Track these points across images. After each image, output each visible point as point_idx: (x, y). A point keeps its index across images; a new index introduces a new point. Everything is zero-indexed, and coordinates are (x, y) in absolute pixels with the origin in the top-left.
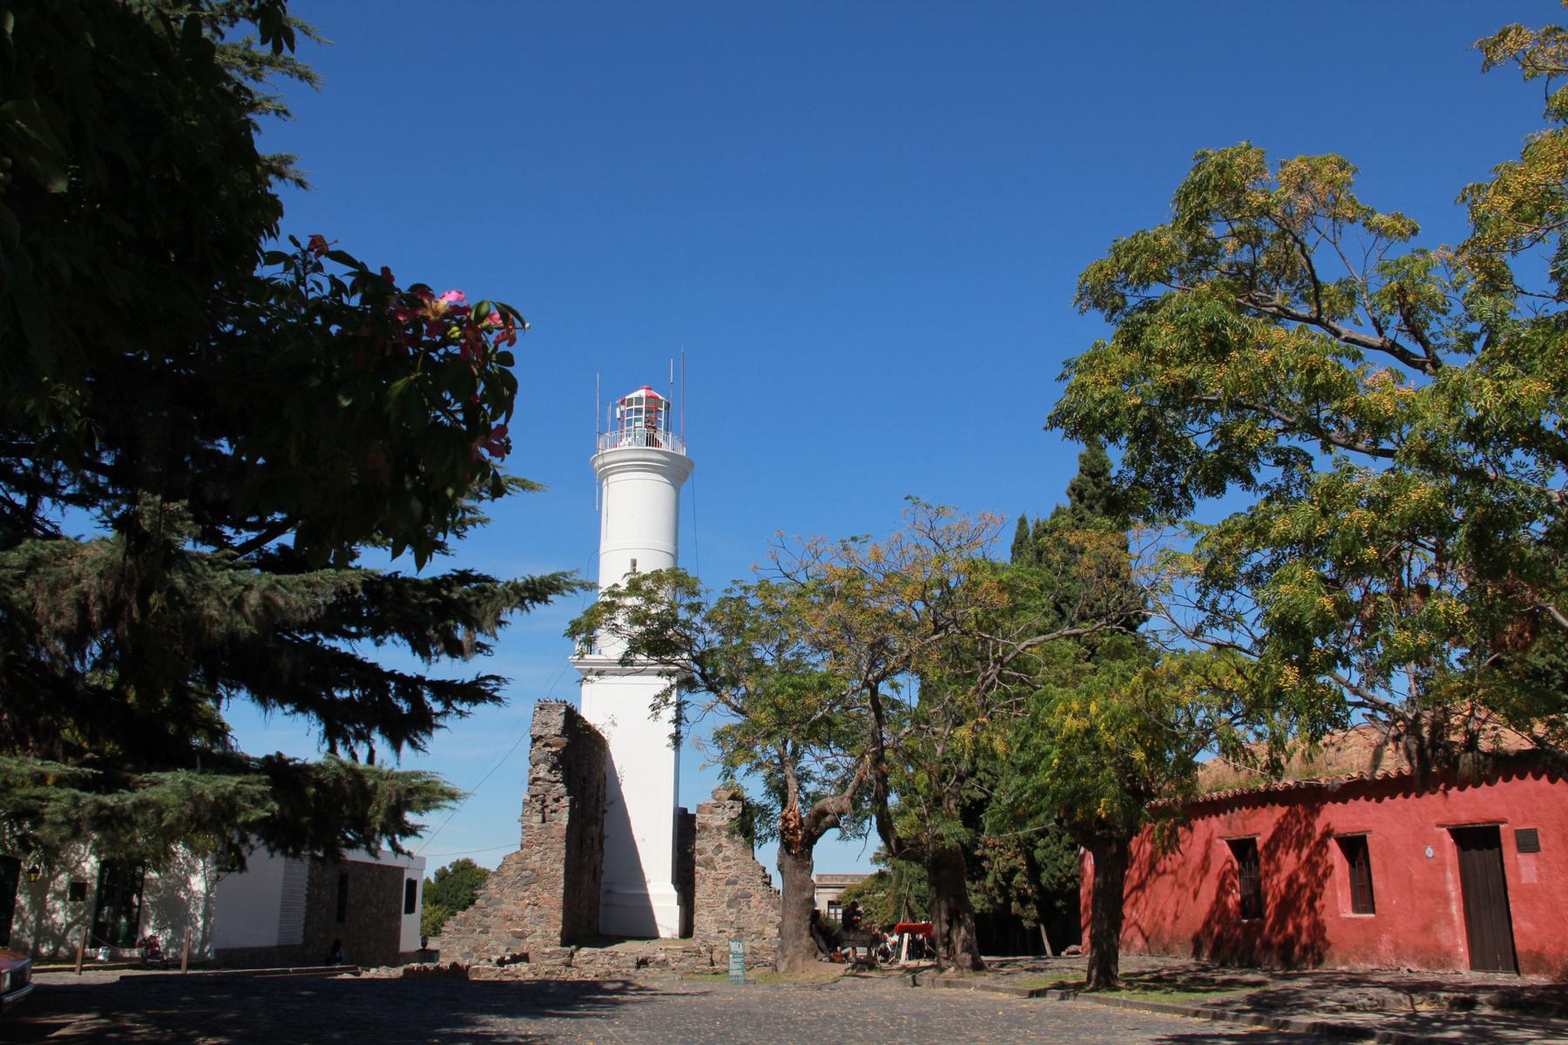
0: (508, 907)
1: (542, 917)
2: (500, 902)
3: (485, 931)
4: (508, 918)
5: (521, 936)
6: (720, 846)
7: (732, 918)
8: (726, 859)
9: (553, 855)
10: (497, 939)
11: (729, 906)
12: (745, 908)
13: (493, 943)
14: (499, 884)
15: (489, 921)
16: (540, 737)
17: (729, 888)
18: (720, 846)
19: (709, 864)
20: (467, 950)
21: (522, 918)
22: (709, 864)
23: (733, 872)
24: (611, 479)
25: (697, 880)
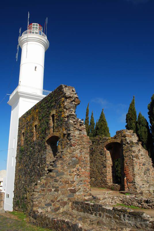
0: (66, 177)
1: (81, 181)
2: (63, 174)
3: (57, 190)
4: (66, 182)
5: (74, 191)
6: (139, 150)
7: (145, 179)
8: (142, 155)
9: (85, 150)
10: (63, 194)
11: (145, 174)
12: (148, 175)
13: (61, 196)
14: (62, 164)
15: (57, 184)
16: (70, 97)
17: (143, 167)
18: (139, 150)
19: (137, 157)
20: (48, 201)
21: (73, 182)
22: (137, 157)
23: (144, 160)
24: (28, 43)
25: (135, 164)
